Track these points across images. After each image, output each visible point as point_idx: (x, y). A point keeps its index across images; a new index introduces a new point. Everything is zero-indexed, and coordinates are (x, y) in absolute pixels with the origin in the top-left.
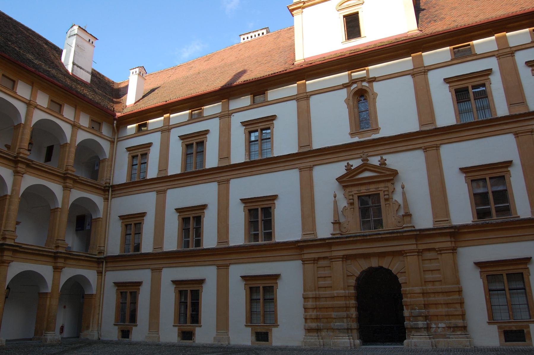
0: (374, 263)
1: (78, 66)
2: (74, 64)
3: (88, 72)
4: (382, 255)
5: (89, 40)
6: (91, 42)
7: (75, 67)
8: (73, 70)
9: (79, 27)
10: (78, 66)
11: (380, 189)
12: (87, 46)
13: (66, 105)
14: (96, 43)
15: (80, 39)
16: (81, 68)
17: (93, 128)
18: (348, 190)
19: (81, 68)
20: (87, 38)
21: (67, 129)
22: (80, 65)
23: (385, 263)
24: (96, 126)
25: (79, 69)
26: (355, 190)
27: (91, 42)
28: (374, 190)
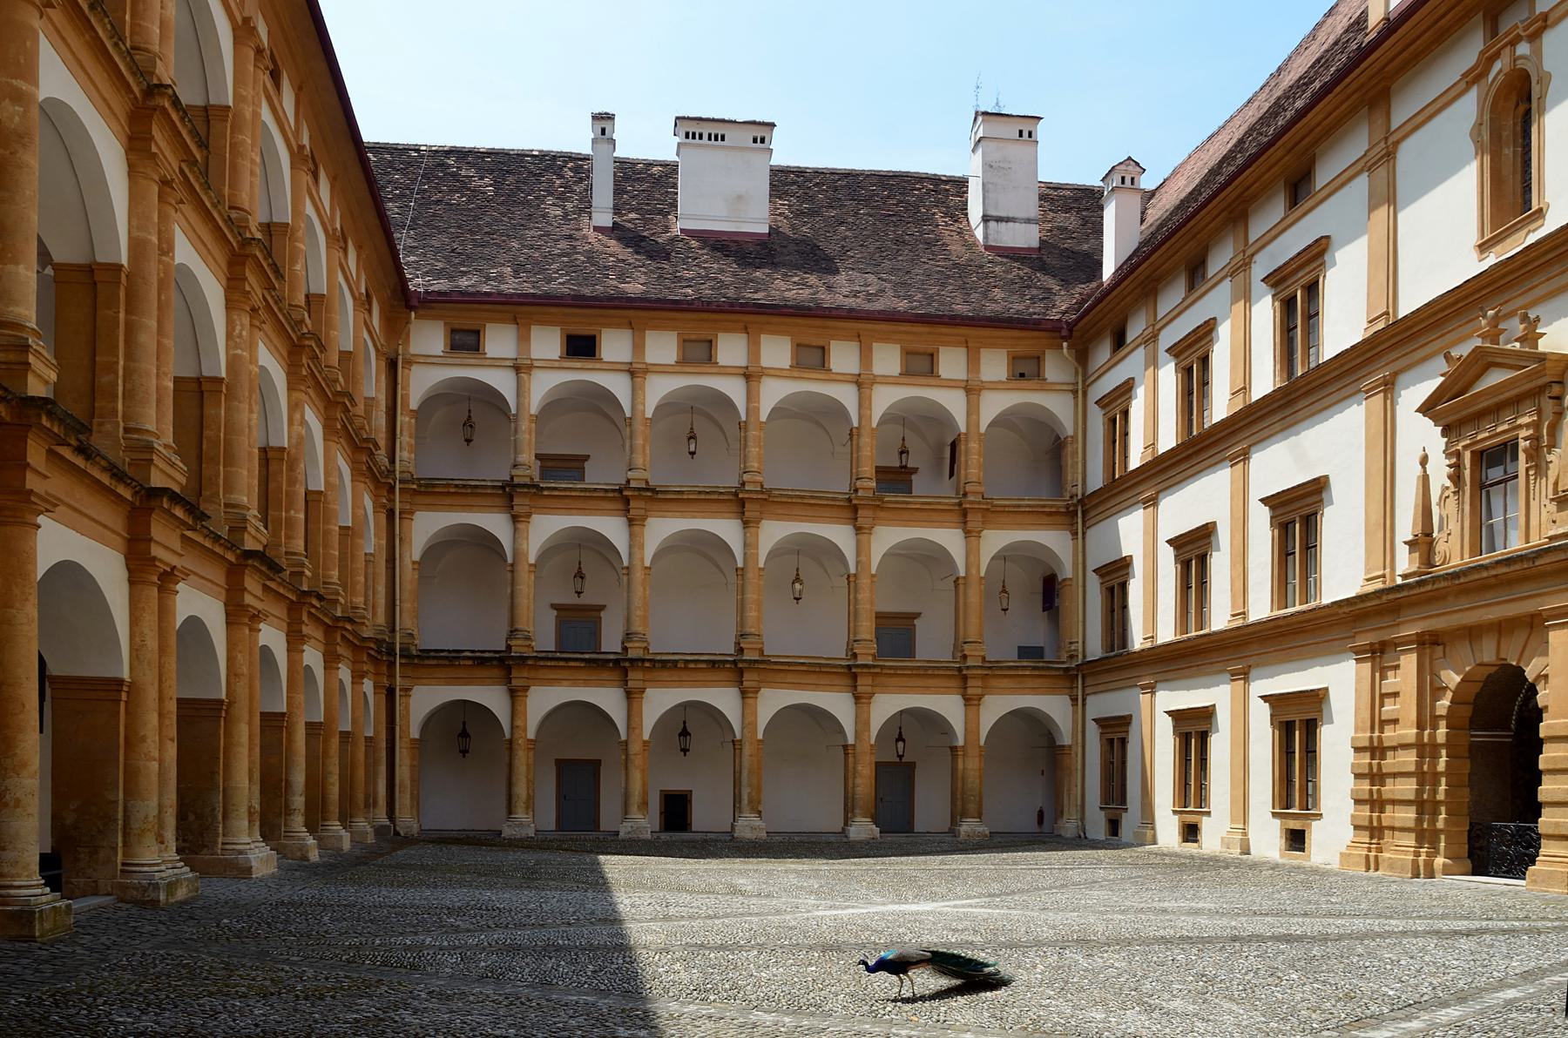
1: (999, 220)
2: (986, 219)
3: (1028, 221)
4: (1503, 628)
6: (1025, 134)
7: (992, 224)
8: (986, 237)
9: (985, 114)
10: (999, 220)
12: (1017, 151)
13: (941, 349)
14: (1041, 130)
15: (992, 145)
16: (1008, 220)
17: (1022, 375)
19: (1008, 220)
21: (954, 403)
22: (1003, 214)
24: (1026, 368)
27: (1025, 134)
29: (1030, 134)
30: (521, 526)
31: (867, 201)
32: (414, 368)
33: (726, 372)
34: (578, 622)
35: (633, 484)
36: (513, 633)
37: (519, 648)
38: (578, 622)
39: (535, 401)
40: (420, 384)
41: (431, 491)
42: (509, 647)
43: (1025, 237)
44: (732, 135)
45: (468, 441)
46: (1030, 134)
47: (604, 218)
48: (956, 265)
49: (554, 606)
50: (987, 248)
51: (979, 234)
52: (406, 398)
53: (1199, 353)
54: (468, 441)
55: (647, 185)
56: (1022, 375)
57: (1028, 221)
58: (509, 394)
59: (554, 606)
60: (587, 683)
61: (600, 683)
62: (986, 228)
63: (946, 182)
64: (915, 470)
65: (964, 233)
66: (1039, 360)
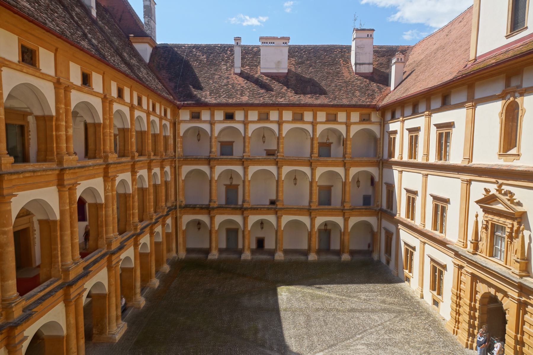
0: (492, 291)
1: (360, 64)
2: (356, 64)
3: (369, 64)
5: (368, 35)
6: (369, 36)
7: (358, 66)
8: (356, 70)
10: (360, 64)
11: (506, 223)
15: (358, 40)
16: (363, 64)
17: (364, 120)
18: (486, 215)
19: (363, 64)
20: (365, 34)
22: (361, 62)
23: (500, 296)
25: (361, 66)
26: (490, 216)
27: (369, 36)
28: (502, 222)
29: (371, 35)
30: (213, 170)
31: (319, 58)
32: (181, 124)
33: (272, 122)
34: (231, 190)
35: (245, 157)
36: (210, 201)
37: (212, 205)
38: (231, 190)
39: (216, 134)
40: (183, 128)
41: (187, 160)
42: (209, 205)
43: (368, 69)
44: (276, 42)
45: (199, 140)
46: (371, 35)
47: (238, 71)
48: (345, 82)
49: (224, 185)
50: (356, 73)
51: (354, 68)
52: (179, 133)
53: (416, 134)
54: (199, 140)
55: (251, 55)
56: (364, 120)
57: (369, 64)
58: (209, 131)
59: (224, 185)
60: (232, 214)
61: (236, 214)
62: (356, 67)
63: (345, 48)
64: (332, 143)
65: (349, 67)
66: (369, 115)
